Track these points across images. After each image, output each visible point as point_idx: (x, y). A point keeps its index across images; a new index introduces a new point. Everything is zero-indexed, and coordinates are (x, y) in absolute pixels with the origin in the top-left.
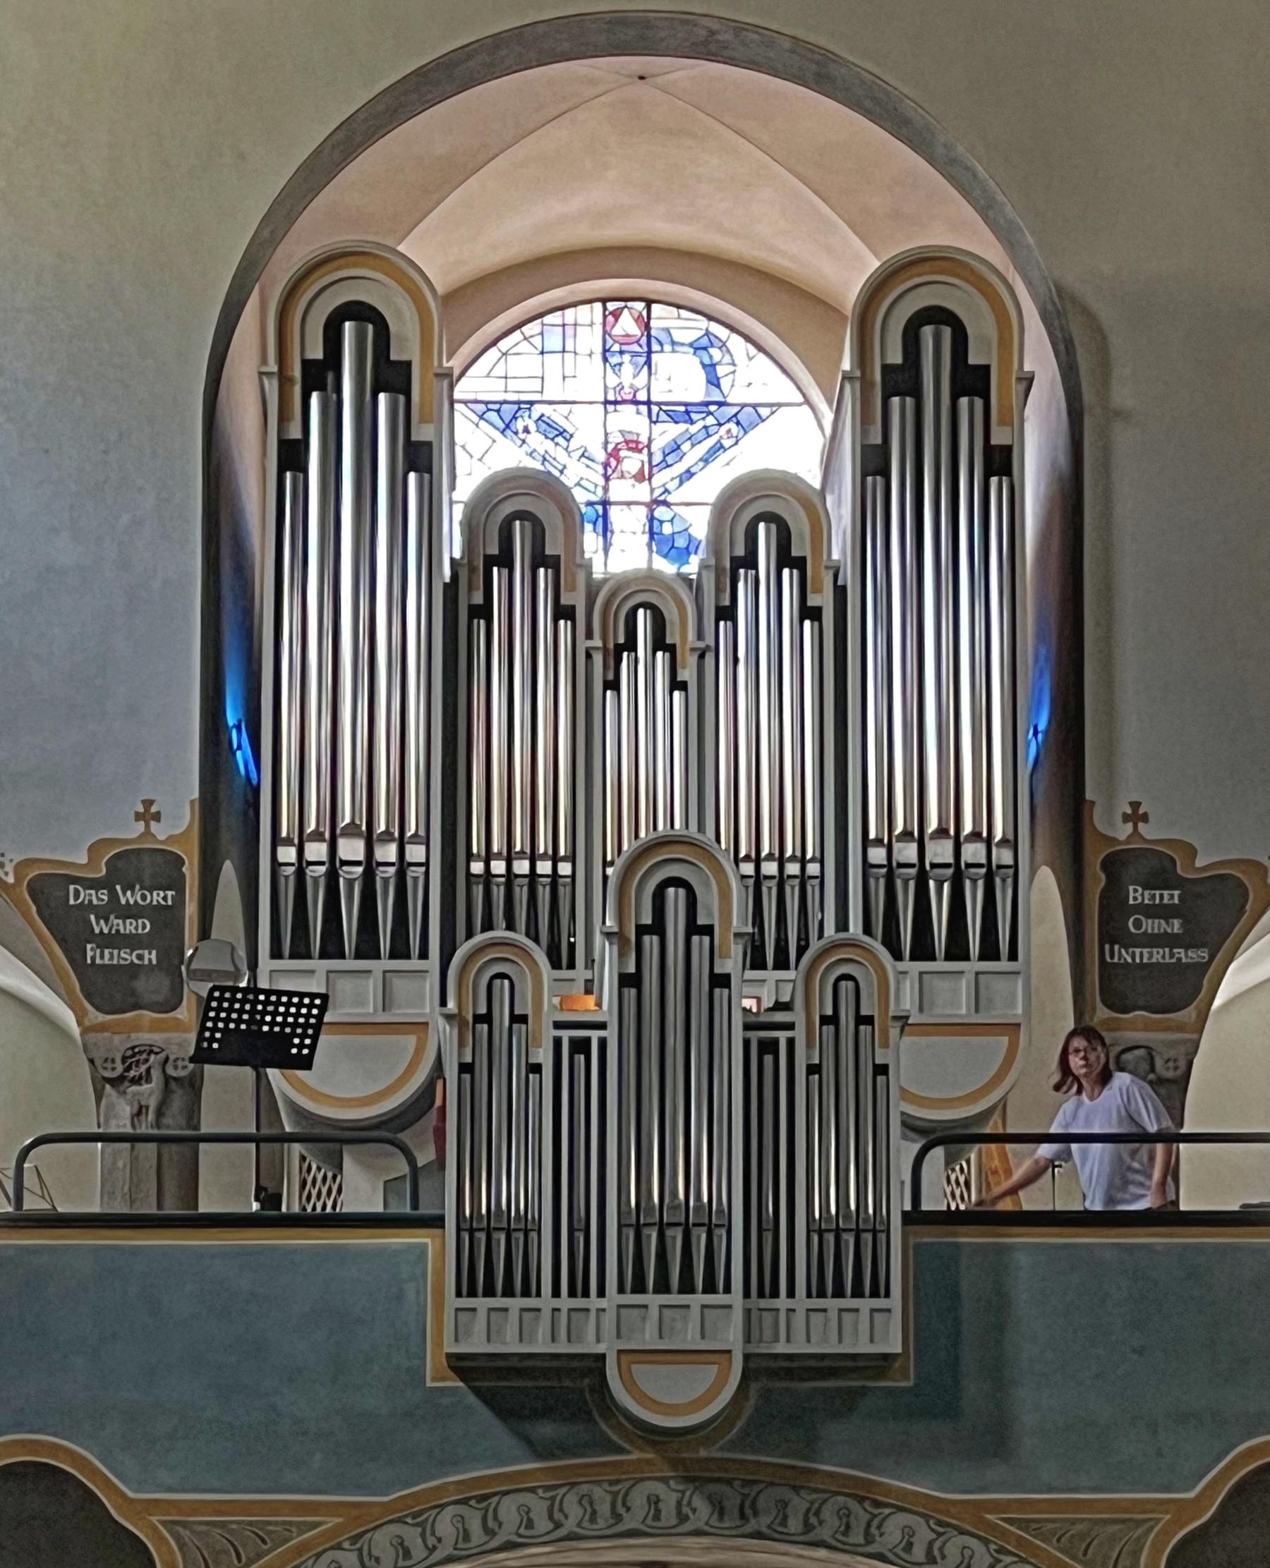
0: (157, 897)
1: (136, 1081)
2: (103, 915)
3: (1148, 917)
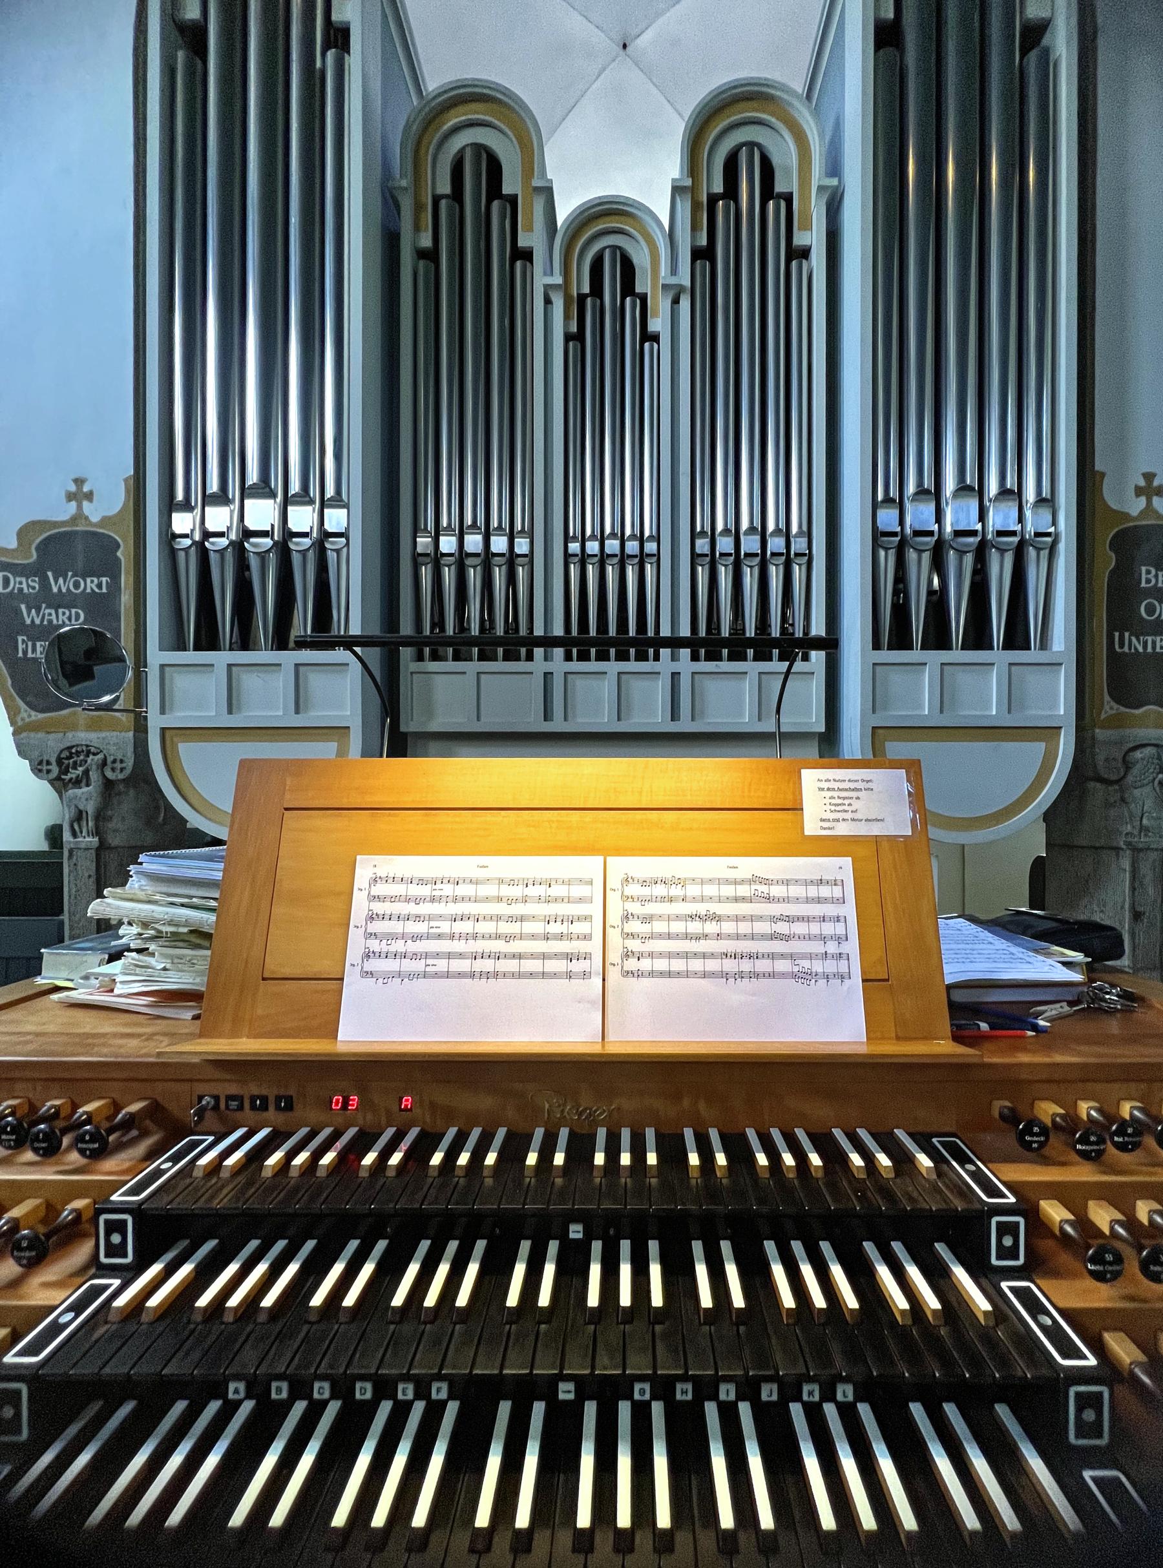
0: (91, 584)
1: (77, 783)
2: (35, 603)
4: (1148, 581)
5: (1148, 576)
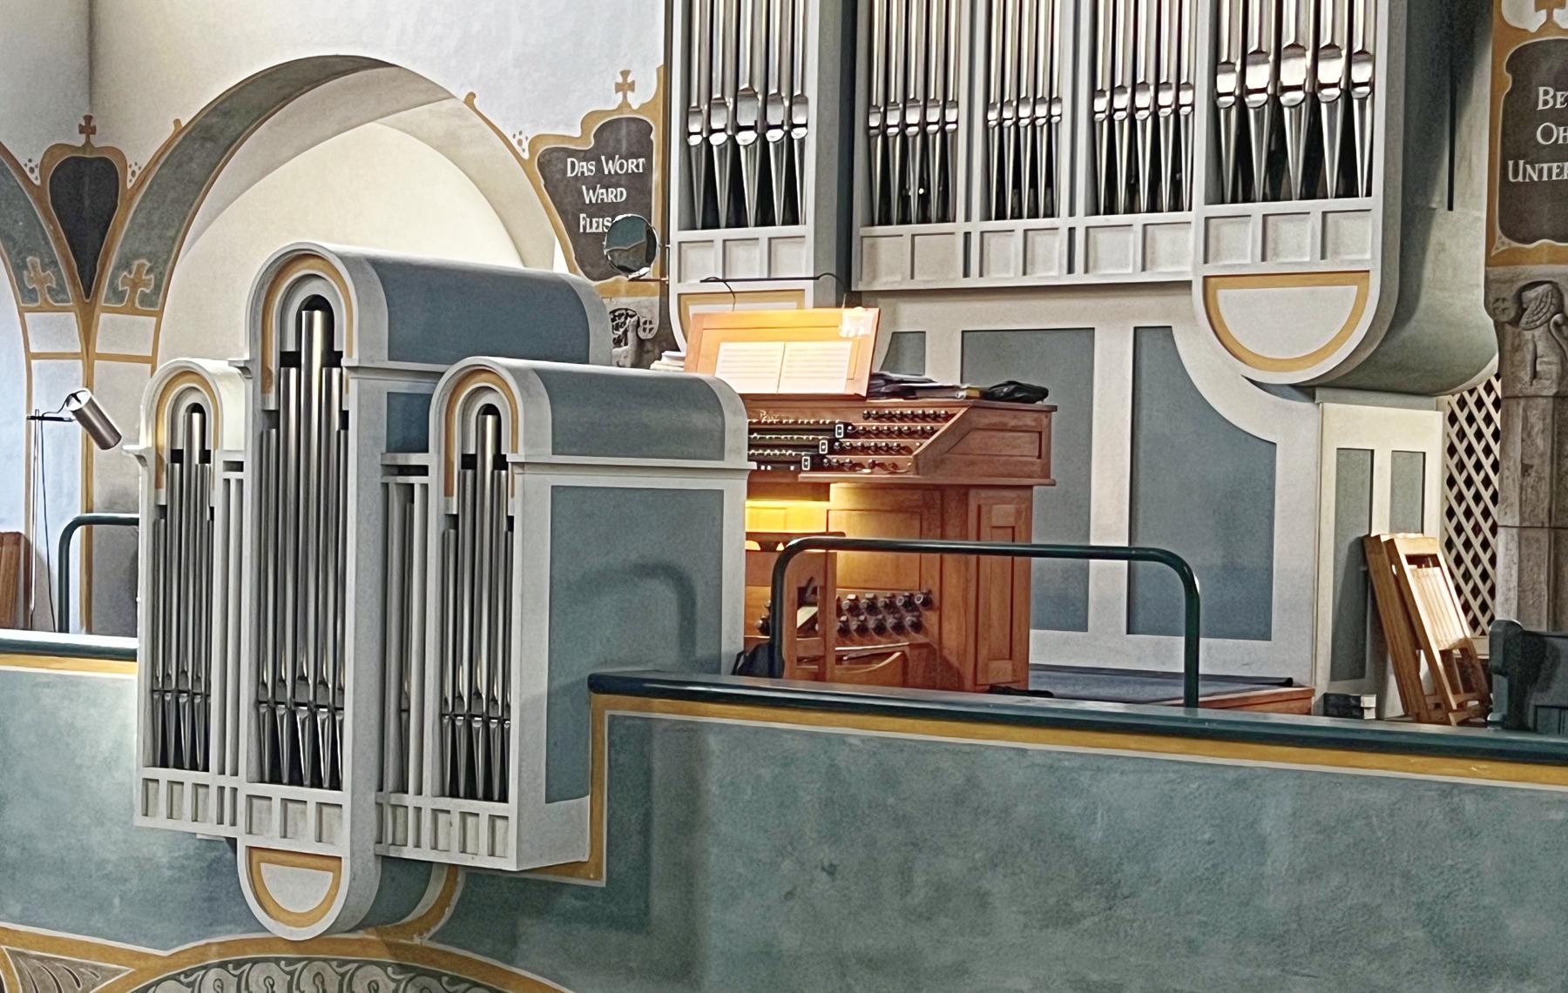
0: (631, 165)
3: (1558, 125)
4: (1546, 103)
5: (1547, 97)
